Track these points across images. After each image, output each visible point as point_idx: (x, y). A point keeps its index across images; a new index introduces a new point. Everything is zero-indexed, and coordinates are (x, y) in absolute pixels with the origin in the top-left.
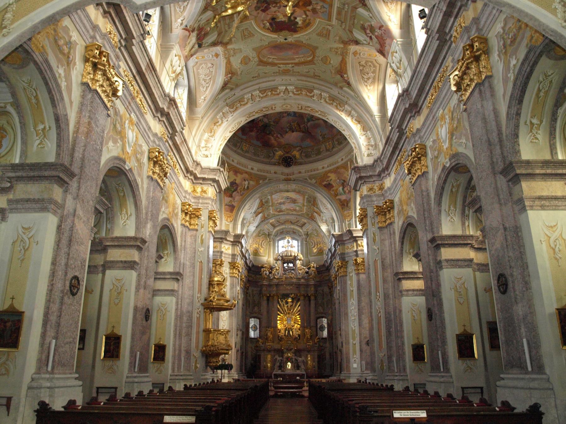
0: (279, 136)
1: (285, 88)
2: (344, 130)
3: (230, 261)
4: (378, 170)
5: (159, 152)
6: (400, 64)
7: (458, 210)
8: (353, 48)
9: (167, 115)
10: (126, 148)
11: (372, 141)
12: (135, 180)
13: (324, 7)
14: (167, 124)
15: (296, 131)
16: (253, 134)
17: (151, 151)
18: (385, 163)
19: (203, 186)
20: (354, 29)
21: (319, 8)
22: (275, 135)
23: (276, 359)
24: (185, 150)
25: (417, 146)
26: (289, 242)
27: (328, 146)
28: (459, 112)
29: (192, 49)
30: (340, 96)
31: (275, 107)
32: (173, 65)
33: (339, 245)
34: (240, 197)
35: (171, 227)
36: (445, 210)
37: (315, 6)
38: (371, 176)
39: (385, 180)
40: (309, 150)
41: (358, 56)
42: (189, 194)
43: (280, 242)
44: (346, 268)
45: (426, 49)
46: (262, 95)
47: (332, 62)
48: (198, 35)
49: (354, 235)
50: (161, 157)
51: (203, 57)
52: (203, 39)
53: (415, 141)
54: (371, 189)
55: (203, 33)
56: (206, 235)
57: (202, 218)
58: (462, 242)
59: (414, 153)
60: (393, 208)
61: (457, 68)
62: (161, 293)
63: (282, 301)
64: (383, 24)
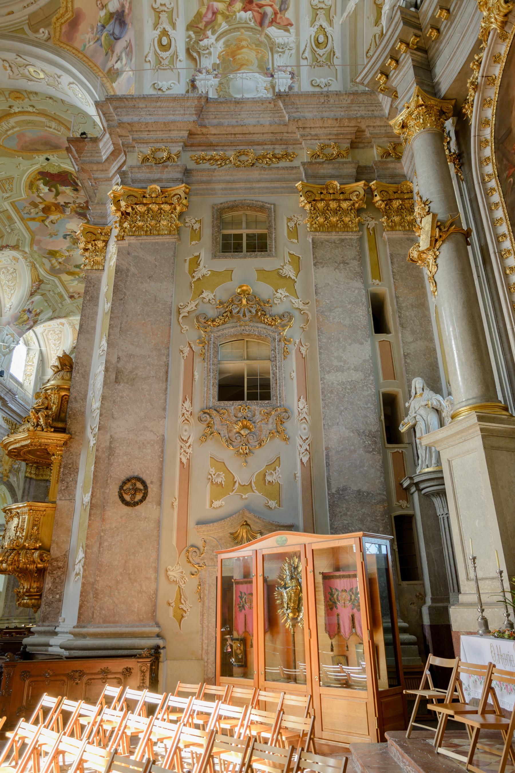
21: (32, 210)
37: (37, 210)
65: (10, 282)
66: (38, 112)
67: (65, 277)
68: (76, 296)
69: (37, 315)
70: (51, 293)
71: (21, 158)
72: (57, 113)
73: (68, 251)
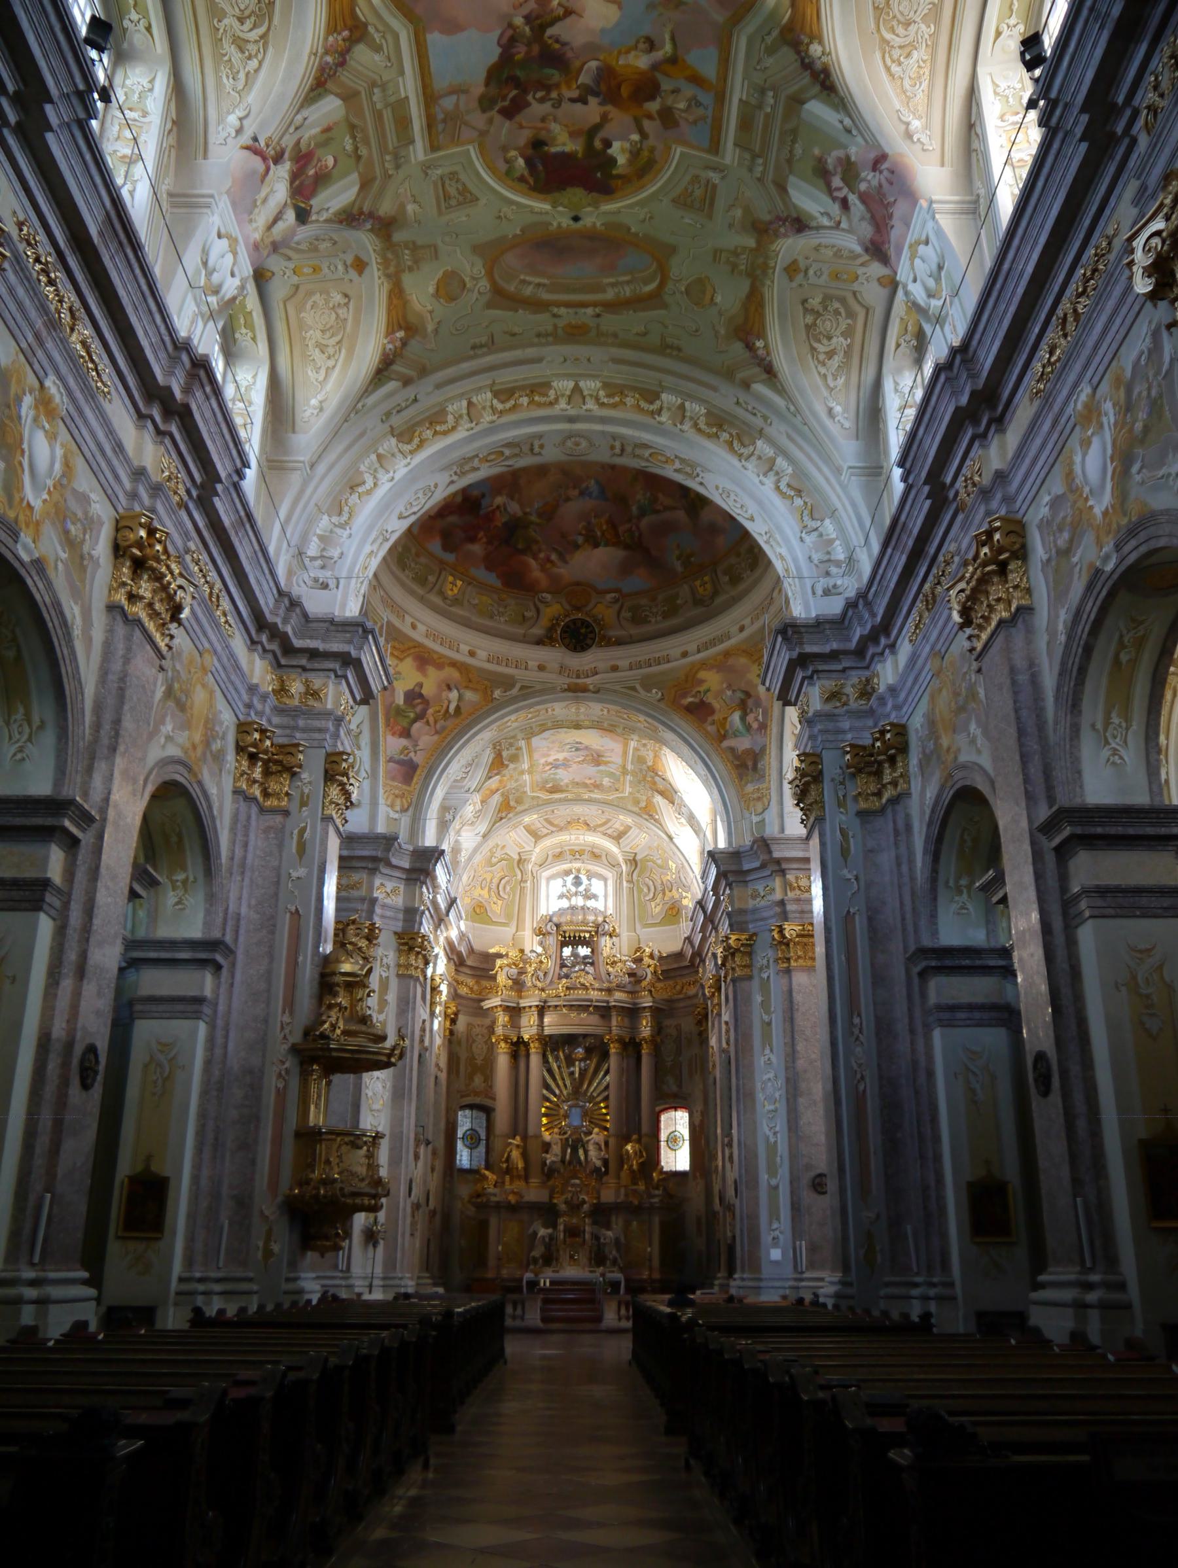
0: (554, 557)
1: (571, 384)
2: (752, 519)
3: (399, 930)
4: (858, 633)
5: (151, 532)
6: (938, 280)
7: (1134, 727)
8: (788, 247)
9: (183, 415)
10: (21, 488)
11: (839, 549)
12: (57, 605)
13: (699, 104)
14: (183, 447)
15: (606, 545)
16: (477, 549)
17: (121, 525)
18: (880, 611)
19: (311, 676)
20: (792, 179)
21: (682, 105)
22: (542, 555)
23: (535, 1233)
24: (249, 550)
25: (998, 524)
26: (577, 882)
27: (701, 590)
28: (1157, 373)
29: (275, 221)
30: (739, 412)
31: (542, 446)
32: (211, 263)
33: (729, 885)
34: (436, 738)
35: (195, 791)
36: (1093, 726)
37: (669, 102)
38: (834, 655)
39: (879, 667)
40: (644, 601)
41: (799, 278)
42: (264, 698)
43: (552, 882)
44: (750, 954)
45: (1040, 184)
46: (500, 406)
47: (718, 299)
48: (294, 176)
49: (776, 855)
50: (158, 547)
51: (316, 270)
52: (313, 193)
53: (988, 513)
54: (833, 696)
55: (311, 172)
56: (314, 828)
57: (305, 775)
58: (1150, 831)
59: (986, 550)
60: (904, 749)
61: (1162, 205)
62: (161, 1008)
63: (557, 1059)
64: (887, 150)
71: (633, 230)
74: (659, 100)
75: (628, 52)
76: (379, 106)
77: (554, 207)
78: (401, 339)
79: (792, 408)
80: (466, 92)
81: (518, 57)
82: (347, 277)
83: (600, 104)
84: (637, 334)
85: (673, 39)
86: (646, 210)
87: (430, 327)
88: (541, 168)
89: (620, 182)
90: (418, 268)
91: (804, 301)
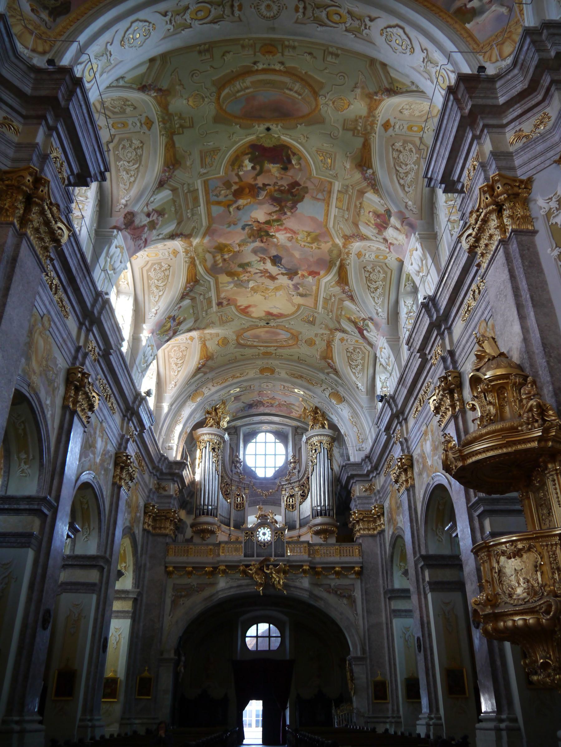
37: (228, 192)
51: (410, 128)
65: (160, 282)
66: (285, 70)
67: (223, 278)
68: (225, 303)
69: (179, 324)
70: (202, 297)
71: (238, 126)
72: (309, 73)
73: (239, 245)
74: (233, 191)
75: (247, 204)
76: (347, 213)
77: (279, 137)
78: (377, 96)
79: (121, 83)
80: (313, 197)
81: (290, 202)
82: (396, 120)
83: (257, 184)
84: (229, 52)
85: (230, 212)
86: (233, 140)
87: (358, 91)
88: (285, 158)
89: (247, 151)
90: (356, 116)
91: (135, 108)
